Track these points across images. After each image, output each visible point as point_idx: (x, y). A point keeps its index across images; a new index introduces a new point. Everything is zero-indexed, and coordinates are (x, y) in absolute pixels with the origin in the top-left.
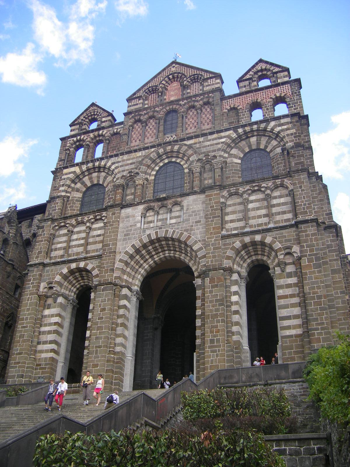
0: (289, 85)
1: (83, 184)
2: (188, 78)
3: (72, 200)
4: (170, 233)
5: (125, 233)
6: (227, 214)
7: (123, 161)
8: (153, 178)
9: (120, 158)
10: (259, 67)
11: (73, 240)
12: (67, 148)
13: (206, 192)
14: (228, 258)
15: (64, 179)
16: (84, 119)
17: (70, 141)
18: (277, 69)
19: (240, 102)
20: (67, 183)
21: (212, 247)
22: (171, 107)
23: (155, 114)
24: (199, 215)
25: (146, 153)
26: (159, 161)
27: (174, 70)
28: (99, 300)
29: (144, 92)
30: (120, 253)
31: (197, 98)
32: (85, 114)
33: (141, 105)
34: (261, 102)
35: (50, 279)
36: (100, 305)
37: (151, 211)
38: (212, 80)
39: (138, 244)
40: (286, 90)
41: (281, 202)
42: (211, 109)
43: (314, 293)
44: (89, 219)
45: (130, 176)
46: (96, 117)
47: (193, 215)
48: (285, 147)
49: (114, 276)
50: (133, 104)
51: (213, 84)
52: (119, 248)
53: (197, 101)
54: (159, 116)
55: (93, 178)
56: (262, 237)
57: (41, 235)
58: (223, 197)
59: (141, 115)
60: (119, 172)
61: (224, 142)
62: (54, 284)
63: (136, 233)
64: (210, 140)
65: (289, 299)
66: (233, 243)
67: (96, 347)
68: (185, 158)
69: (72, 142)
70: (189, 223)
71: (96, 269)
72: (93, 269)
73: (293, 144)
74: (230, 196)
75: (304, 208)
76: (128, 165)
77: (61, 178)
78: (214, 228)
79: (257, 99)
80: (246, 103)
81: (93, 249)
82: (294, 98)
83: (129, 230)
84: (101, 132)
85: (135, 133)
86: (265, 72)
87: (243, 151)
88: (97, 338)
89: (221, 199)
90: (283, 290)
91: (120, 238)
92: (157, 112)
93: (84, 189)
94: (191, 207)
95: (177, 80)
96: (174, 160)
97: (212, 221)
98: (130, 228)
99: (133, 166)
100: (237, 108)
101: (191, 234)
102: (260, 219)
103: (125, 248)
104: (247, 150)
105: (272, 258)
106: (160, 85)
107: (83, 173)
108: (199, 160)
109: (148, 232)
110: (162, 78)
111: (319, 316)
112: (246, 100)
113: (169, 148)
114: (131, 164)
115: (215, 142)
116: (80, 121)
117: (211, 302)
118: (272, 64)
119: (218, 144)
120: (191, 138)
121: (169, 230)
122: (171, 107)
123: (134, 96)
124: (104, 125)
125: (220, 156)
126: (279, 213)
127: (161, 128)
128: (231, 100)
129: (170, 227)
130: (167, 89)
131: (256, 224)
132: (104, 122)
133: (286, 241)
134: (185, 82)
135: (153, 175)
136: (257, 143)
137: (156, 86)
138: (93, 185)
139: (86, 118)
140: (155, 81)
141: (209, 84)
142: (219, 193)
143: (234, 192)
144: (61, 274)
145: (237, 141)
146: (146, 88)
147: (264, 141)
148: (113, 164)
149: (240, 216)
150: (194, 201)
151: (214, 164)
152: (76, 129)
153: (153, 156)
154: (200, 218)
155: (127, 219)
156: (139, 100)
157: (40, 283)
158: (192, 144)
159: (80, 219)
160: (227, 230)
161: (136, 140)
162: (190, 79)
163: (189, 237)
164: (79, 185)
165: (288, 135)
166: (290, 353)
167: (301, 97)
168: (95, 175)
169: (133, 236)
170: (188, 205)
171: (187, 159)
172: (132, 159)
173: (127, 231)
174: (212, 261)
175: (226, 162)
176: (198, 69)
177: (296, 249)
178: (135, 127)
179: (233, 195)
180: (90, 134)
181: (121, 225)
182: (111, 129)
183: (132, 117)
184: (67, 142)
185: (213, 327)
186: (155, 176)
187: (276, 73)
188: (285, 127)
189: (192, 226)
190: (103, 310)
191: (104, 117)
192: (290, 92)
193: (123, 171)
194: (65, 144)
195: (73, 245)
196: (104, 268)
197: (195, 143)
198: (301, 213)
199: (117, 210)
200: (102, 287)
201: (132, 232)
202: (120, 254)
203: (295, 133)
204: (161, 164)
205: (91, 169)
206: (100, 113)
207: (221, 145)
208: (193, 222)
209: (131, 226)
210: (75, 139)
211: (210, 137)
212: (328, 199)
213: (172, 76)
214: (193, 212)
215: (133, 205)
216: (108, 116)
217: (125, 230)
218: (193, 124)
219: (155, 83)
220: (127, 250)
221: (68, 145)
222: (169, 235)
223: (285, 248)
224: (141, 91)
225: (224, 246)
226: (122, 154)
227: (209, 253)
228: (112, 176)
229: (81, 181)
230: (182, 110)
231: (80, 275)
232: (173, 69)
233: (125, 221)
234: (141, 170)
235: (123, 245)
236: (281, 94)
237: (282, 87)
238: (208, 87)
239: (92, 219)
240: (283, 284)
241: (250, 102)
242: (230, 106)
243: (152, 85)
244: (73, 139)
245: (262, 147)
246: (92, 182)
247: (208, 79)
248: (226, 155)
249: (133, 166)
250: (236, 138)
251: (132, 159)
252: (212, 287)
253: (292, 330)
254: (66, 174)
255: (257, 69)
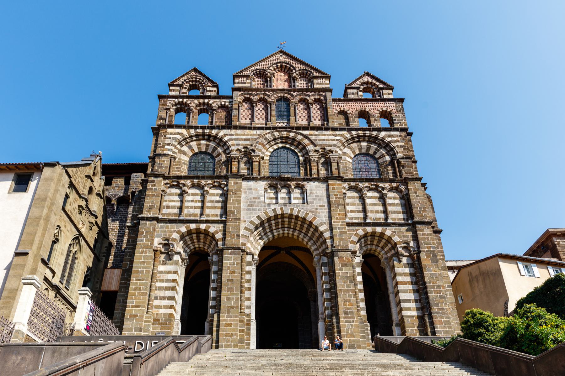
0: (394, 103)
1: (190, 148)
2: (298, 71)
3: (180, 162)
4: (295, 211)
5: (248, 203)
6: (348, 204)
7: (237, 135)
8: (268, 158)
9: (233, 132)
10: (366, 79)
11: (189, 201)
12: (167, 107)
13: (329, 181)
14: (352, 242)
15: (170, 138)
16: (185, 82)
17: (170, 101)
18: (381, 86)
19: (349, 107)
20: (173, 143)
21: (339, 231)
22: (282, 95)
23: (266, 97)
24: (322, 200)
25: (260, 132)
26: (274, 143)
27: (282, 59)
28: (227, 263)
29: (252, 72)
30: (245, 221)
31: (308, 93)
32: (185, 78)
33: (249, 85)
34: (369, 112)
35: (166, 235)
36: (229, 268)
37: (273, 188)
38: (321, 79)
39: (264, 217)
40: (391, 107)
41: (396, 203)
42: (321, 107)
43: (433, 283)
44: (207, 183)
45: (244, 151)
46: (197, 84)
47: (317, 199)
48: (394, 156)
49: (240, 242)
50: (240, 81)
51: (323, 84)
52: (244, 217)
53: (309, 96)
54: (271, 100)
55: (202, 145)
56: (382, 229)
57: (151, 189)
58: (344, 188)
59: (251, 95)
60: (233, 145)
61: (339, 140)
62: (171, 241)
63: (260, 206)
64: (325, 135)
65: (408, 285)
66: (357, 230)
67: (228, 307)
68: (301, 147)
69: (172, 102)
70: (314, 206)
71: (220, 233)
72: (217, 232)
73: (403, 156)
74: (349, 189)
75: (420, 212)
76: (241, 139)
77: (165, 136)
78: (339, 214)
79: (365, 108)
80: (355, 109)
81: (213, 213)
82: (399, 115)
83: (252, 201)
84: (206, 101)
85: (244, 110)
86: (370, 86)
87: (354, 152)
88: (228, 299)
89: (343, 190)
90: (402, 277)
91: (243, 207)
92: (269, 96)
93: (191, 154)
94: (315, 192)
95: (284, 70)
96: (288, 146)
97: (337, 207)
98: (254, 200)
99: (248, 142)
100: (346, 112)
101: (316, 216)
102: (378, 214)
103: (250, 218)
104: (357, 152)
105: (386, 250)
106: (268, 70)
107: (191, 137)
108: (316, 151)
109: (273, 207)
110: (270, 64)
111: (439, 302)
112: (355, 106)
113: (284, 133)
114: (246, 140)
115: (330, 138)
116: (180, 83)
117: (342, 278)
118: (378, 80)
119: (334, 140)
120: (305, 129)
121: (294, 209)
122: (282, 95)
123: (241, 74)
124: (208, 94)
125: (336, 152)
126: (394, 212)
127: (274, 113)
128: (340, 103)
129: (295, 206)
130: (274, 76)
131: (374, 217)
132: (210, 91)
133: (404, 236)
134: (295, 75)
135: (267, 156)
136: (367, 148)
137: (265, 70)
138: (201, 153)
139: (187, 83)
140: (263, 65)
141: (319, 82)
142: (341, 184)
143: (353, 186)
144: (179, 232)
145: (350, 142)
146: (253, 69)
147: (374, 147)
148: (226, 135)
149: (359, 208)
150: (316, 187)
151: (331, 158)
152: (177, 90)
153: (269, 137)
154: (323, 202)
155: (250, 191)
156: (247, 79)
157: (153, 237)
158: (307, 134)
159: (196, 181)
160: (350, 218)
161: (246, 118)
162: (299, 73)
163: (314, 218)
164: (185, 148)
165: (398, 146)
166: (412, 330)
167: (405, 115)
168: (203, 142)
169: (258, 208)
170: (311, 190)
171: (302, 148)
172: (247, 135)
173: (250, 202)
174: (340, 243)
175: (340, 158)
176: (307, 65)
177: (412, 244)
178: (244, 105)
179: (351, 189)
180: (193, 100)
181: (243, 196)
182: (218, 100)
183: (242, 94)
184: (167, 101)
185: (345, 300)
186: (270, 156)
187: (382, 89)
188: (394, 139)
189: (317, 209)
190: (233, 272)
191: (209, 86)
192: (395, 109)
193: (239, 145)
194: (164, 103)
195: (189, 206)
196: (230, 232)
197: (311, 135)
198: (418, 215)
199: (239, 180)
200: (230, 251)
201: (256, 204)
202: (245, 223)
203: (405, 146)
204: (275, 147)
205: (200, 135)
206: (203, 81)
207: (337, 142)
208: (317, 206)
209: (254, 198)
210: (176, 100)
211: (325, 132)
212: (433, 208)
213: (281, 65)
214: (316, 196)
215: (255, 179)
216: (213, 86)
217: (248, 201)
218: (304, 116)
219: (262, 66)
220: (252, 219)
221: (168, 104)
222: (295, 213)
223: (403, 242)
224: (248, 71)
225: (349, 232)
226: (236, 128)
227: (336, 235)
228: (224, 147)
229: (187, 145)
230: (294, 101)
231: (197, 236)
232: (281, 58)
233: (248, 192)
234: (257, 148)
235: (248, 215)
236: (387, 109)
237: (388, 103)
238: (318, 85)
239: (210, 184)
240: (401, 272)
241: (358, 109)
242: (340, 108)
243: (260, 68)
244: (173, 99)
245: (371, 152)
246: (199, 148)
247: (317, 77)
248: (340, 152)
249: (248, 142)
250: (350, 139)
251: (247, 135)
252: (342, 265)
253: (412, 311)
254: (171, 134)
255: (363, 80)
